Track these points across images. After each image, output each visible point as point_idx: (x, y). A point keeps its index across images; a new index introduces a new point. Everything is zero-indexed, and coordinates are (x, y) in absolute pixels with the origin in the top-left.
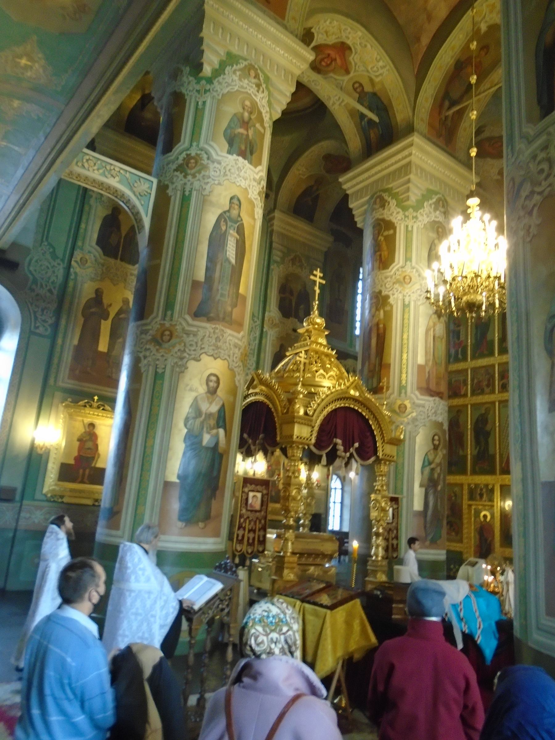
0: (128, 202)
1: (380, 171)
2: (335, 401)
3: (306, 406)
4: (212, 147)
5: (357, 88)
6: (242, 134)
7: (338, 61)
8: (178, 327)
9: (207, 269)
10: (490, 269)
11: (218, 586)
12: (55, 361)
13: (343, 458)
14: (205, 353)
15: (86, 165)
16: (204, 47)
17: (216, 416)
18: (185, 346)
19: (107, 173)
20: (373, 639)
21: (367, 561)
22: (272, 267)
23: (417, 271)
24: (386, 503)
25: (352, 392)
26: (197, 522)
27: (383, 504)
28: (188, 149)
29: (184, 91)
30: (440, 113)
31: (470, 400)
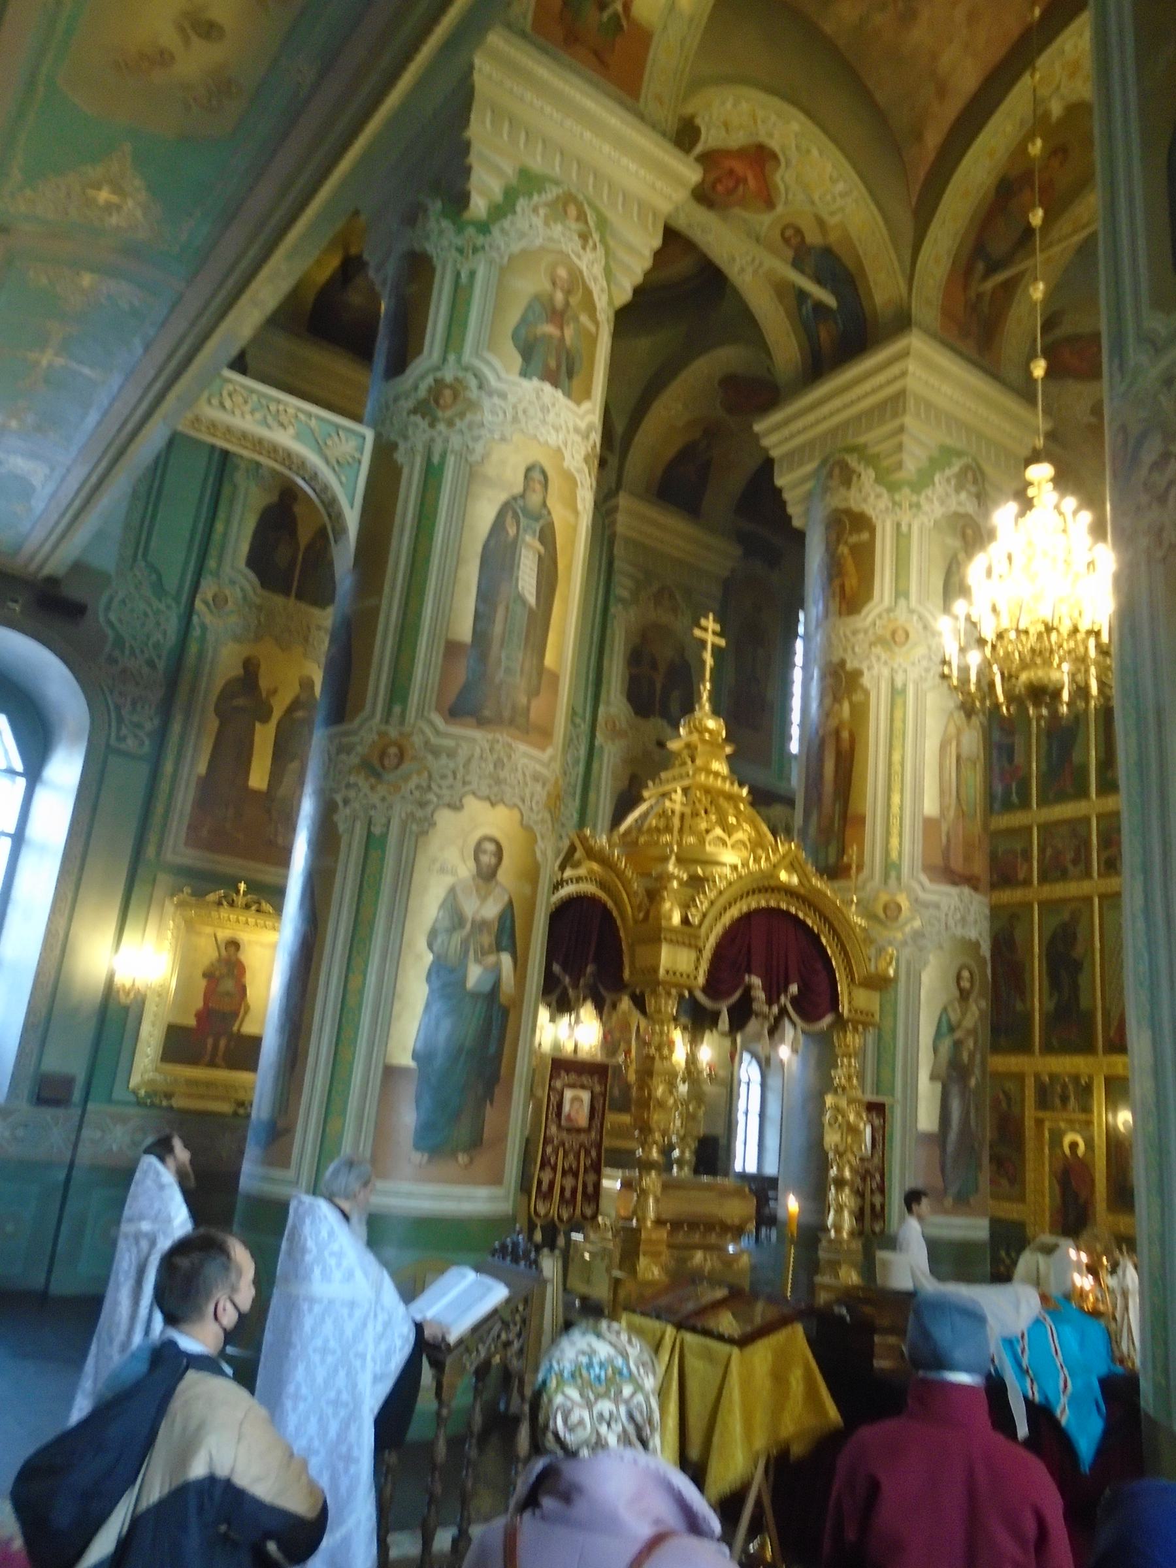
0: (312, 478)
1: (838, 411)
2: (748, 894)
3: (686, 906)
4: (488, 363)
6: (551, 337)
7: (752, 182)
8: (417, 740)
9: (477, 616)
10: (1076, 615)
11: (498, 1294)
12: (159, 808)
13: (766, 1017)
14: (474, 794)
15: (228, 403)
16: (473, 159)
18: (430, 777)
19: (270, 419)
20: (833, 1411)
21: (818, 1240)
22: (613, 610)
23: (921, 618)
24: (858, 1115)
25: (783, 876)
26: (453, 1154)
27: (852, 1118)
28: (438, 369)
29: (430, 248)
30: (966, 287)
31: (1038, 892)
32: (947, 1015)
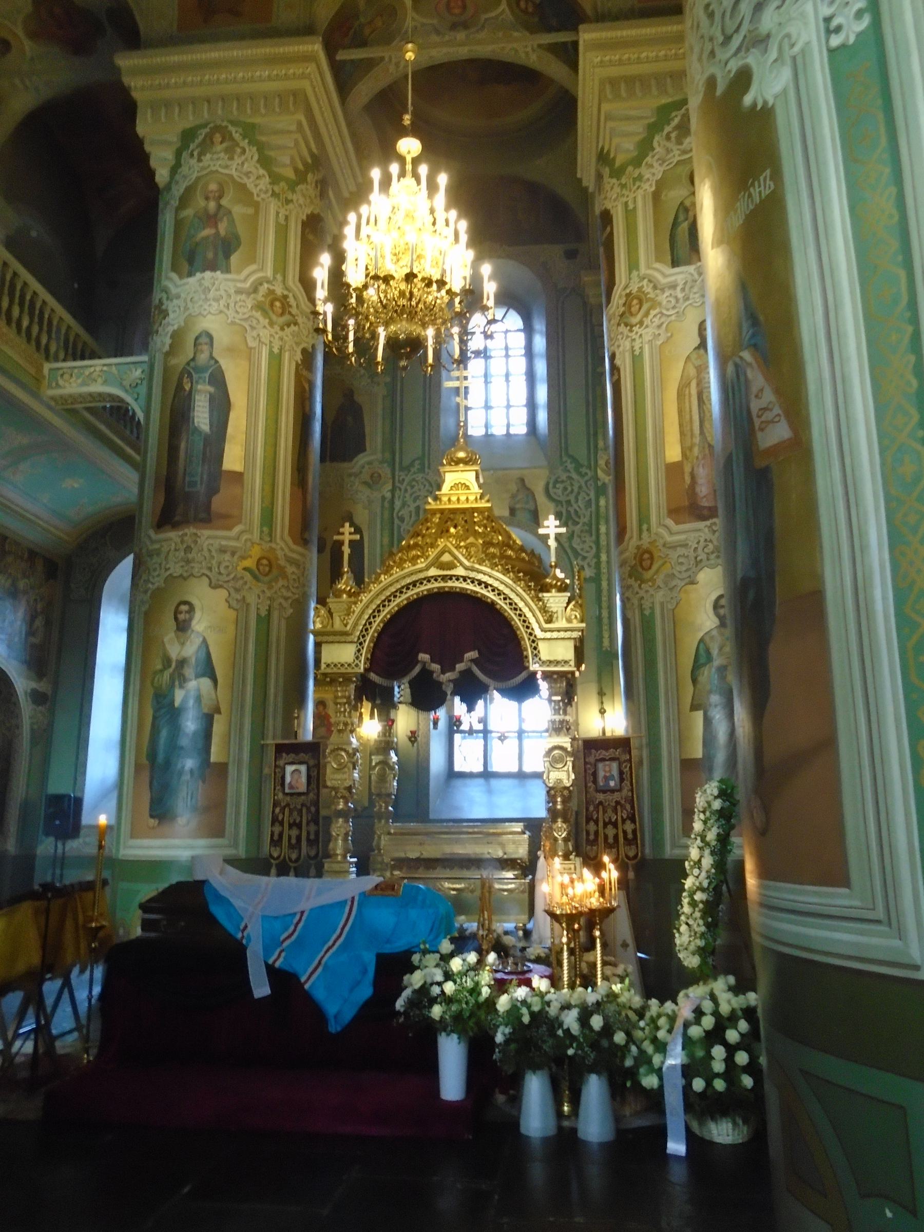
5: (526, 8)
6: (207, 238)
15: (61, 382)
16: (147, 148)
17: (193, 660)
32: (705, 644)
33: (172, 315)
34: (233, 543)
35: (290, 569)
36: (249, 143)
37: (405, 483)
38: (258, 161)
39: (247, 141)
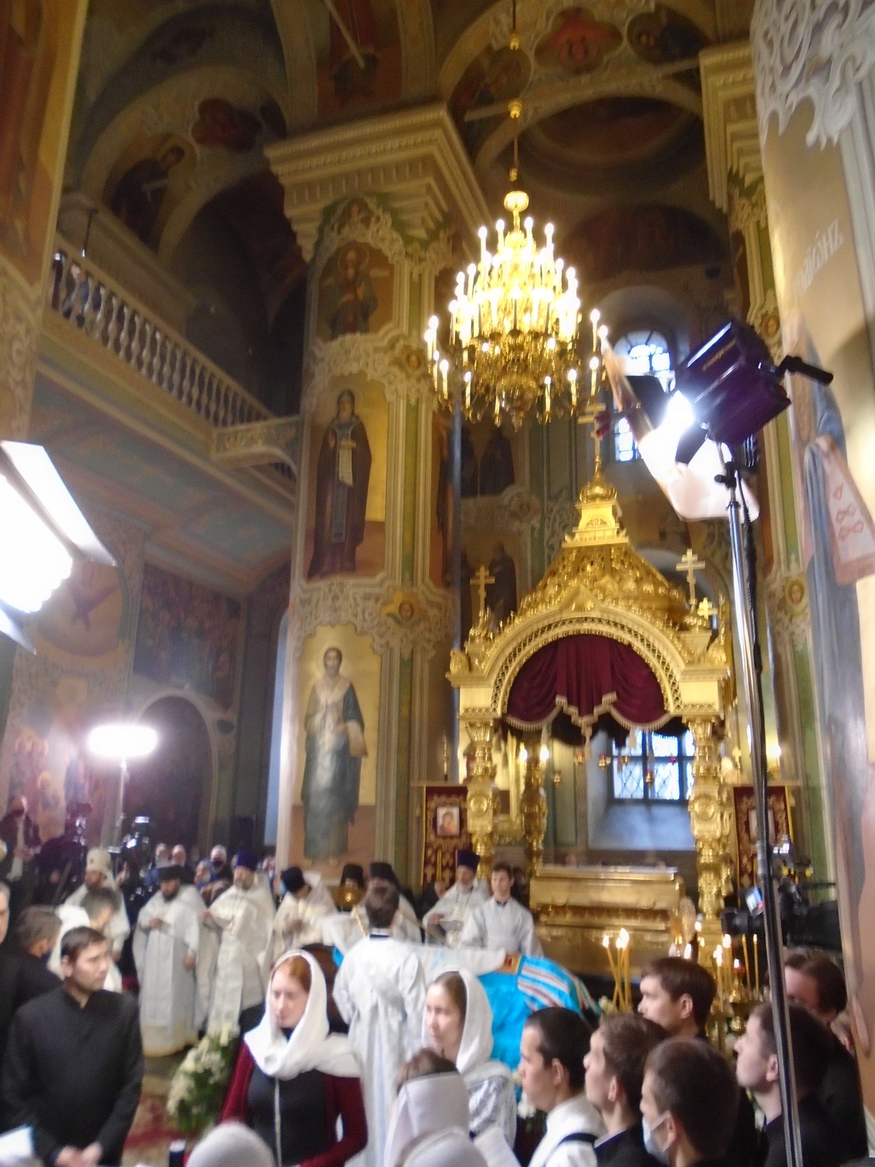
15: (228, 445)
16: (295, 227)
33: (317, 379)
34: (376, 591)
35: (433, 612)
36: (383, 211)
37: (553, 513)
38: (393, 225)
39: (381, 210)
